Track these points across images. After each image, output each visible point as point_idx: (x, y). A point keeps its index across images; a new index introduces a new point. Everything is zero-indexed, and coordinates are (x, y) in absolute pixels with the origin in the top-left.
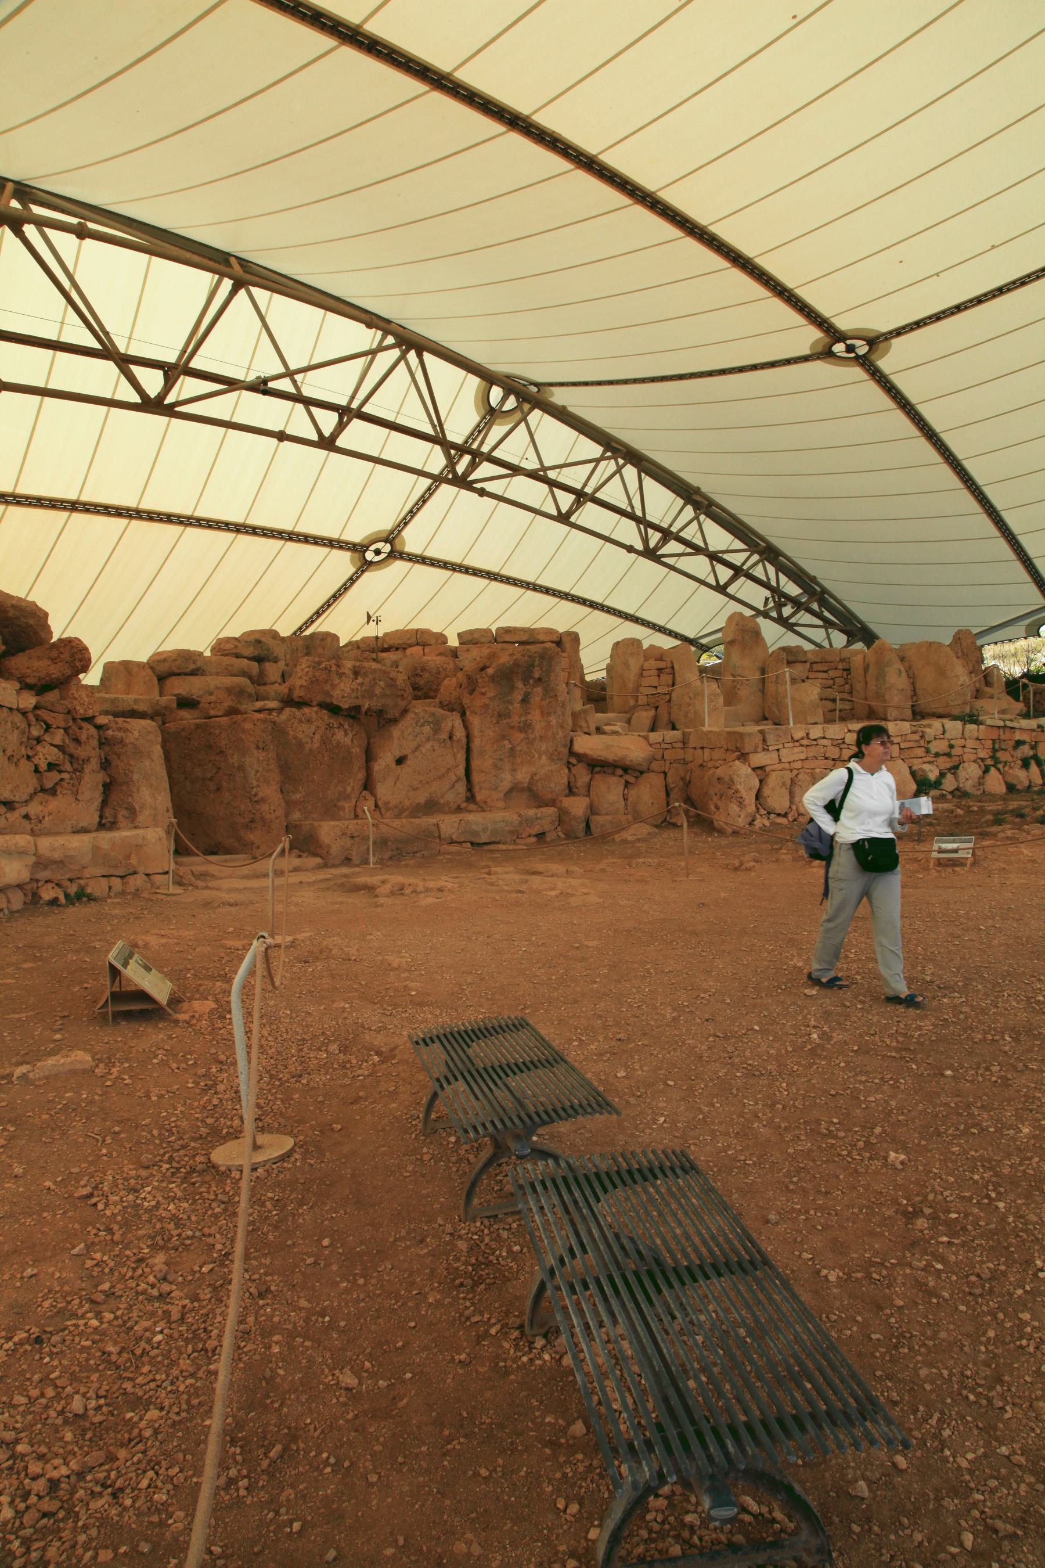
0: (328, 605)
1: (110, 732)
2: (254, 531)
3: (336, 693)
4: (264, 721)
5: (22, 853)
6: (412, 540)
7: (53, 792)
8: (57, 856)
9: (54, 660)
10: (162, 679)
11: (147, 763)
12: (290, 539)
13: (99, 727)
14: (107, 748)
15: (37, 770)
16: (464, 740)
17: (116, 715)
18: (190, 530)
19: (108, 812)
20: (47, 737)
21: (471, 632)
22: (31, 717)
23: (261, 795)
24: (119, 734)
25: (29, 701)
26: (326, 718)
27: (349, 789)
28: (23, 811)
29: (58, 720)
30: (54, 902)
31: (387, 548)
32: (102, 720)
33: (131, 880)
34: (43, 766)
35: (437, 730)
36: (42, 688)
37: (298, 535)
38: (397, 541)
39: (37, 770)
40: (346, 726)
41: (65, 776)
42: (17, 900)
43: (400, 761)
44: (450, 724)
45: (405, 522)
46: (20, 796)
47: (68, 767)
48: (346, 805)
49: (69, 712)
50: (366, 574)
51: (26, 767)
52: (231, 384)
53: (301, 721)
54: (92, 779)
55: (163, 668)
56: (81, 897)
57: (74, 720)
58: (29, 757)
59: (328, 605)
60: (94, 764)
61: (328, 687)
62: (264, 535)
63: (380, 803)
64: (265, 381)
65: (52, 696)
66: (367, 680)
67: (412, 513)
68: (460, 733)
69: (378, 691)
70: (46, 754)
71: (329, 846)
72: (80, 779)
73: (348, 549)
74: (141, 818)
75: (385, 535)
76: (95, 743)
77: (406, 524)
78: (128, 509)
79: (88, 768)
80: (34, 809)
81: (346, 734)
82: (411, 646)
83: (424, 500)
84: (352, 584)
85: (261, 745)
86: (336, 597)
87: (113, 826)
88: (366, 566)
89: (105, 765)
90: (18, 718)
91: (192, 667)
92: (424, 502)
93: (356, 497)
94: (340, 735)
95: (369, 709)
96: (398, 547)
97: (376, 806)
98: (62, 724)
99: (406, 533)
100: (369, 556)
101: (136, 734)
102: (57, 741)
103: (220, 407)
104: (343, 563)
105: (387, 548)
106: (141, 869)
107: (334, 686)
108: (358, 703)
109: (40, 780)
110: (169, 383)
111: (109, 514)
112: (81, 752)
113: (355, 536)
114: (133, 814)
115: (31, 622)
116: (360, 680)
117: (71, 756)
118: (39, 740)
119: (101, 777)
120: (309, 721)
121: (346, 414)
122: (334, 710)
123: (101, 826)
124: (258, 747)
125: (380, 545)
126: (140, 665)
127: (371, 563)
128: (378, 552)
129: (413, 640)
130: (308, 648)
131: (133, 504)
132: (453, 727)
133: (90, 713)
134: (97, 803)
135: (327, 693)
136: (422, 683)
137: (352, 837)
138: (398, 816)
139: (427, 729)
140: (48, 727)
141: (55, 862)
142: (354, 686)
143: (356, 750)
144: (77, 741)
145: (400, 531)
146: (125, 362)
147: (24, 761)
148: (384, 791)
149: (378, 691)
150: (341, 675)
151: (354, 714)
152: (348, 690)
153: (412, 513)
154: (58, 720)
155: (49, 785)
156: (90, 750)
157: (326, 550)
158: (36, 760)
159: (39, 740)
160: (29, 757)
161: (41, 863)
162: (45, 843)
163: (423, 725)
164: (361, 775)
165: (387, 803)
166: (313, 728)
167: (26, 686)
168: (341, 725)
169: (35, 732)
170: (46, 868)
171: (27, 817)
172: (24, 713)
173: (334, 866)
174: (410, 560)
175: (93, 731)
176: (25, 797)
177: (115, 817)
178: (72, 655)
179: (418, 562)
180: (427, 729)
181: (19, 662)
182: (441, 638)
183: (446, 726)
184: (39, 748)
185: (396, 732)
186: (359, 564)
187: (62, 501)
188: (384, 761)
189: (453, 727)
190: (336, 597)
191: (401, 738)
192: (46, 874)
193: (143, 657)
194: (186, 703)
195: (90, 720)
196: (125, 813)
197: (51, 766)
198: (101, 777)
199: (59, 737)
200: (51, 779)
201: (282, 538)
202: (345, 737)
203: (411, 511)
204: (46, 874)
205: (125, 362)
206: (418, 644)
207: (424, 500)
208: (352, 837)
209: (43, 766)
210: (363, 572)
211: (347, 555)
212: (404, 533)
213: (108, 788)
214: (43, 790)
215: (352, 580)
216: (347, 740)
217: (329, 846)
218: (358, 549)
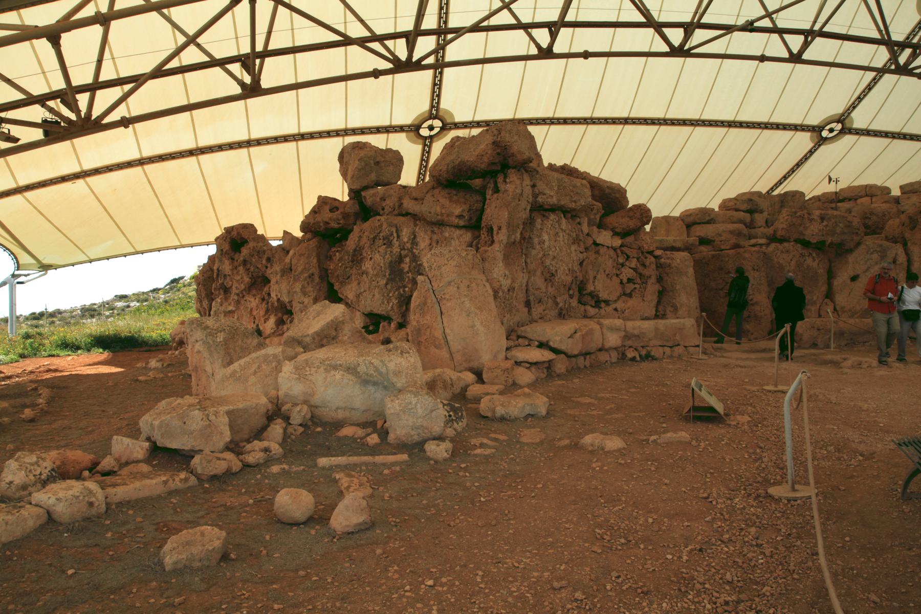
0: (792, 171)
1: (663, 260)
3: (808, 232)
4: (758, 252)
5: (618, 330)
6: (859, 119)
7: (630, 295)
8: (636, 332)
9: (631, 218)
10: (689, 226)
11: (685, 279)
12: (766, 128)
13: (656, 257)
14: (660, 270)
15: (621, 283)
16: (905, 264)
17: (665, 249)
18: (698, 129)
19: (661, 308)
20: (627, 263)
21: (911, 184)
22: (618, 251)
23: (755, 300)
24: (668, 261)
25: (617, 242)
26: (800, 249)
27: (815, 298)
28: (614, 306)
29: (633, 253)
30: (633, 359)
31: (839, 126)
32: (658, 253)
33: (676, 349)
34: (625, 280)
35: (883, 258)
36: (624, 234)
37: (772, 124)
38: (846, 121)
39: (621, 283)
40: (814, 255)
41: (637, 286)
42: (614, 356)
44: (894, 252)
45: (853, 106)
46: (613, 297)
47: (638, 281)
48: (813, 308)
49: (640, 248)
50: (822, 147)
51: (616, 281)
52: (728, 29)
53: (782, 252)
54: (652, 288)
55: (690, 220)
56: (648, 357)
57: (642, 253)
58: (617, 275)
59: (792, 171)
60: (653, 279)
61: (801, 229)
62: (748, 127)
63: (838, 308)
64: (752, 23)
65: (630, 239)
66: (831, 223)
67: (860, 99)
68: (902, 258)
69: (838, 230)
70: (627, 273)
71: (802, 335)
72: (645, 288)
73: (809, 131)
74: (680, 312)
75: (837, 117)
76: (654, 266)
77: (854, 108)
78: (659, 119)
79: (650, 281)
80: (619, 305)
81: (814, 260)
82: (861, 197)
83: (869, 88)
84: (811, 155)
85: (756, 268)
86: (798, 165)
87: (663, 317)
89: (660, 280)
90: (612, 252)
91: (708, 218)
92: (870, 89)
93: (814, 93)
94: (809, 261)
95: (832, 243)
96: (848, 125)
97: (835, 309)
98: (636, 256)
99: (854, 115)
100: (825, 134)
101: (678, 261)
102: (633, 265)
104: (804, 140)
105: (839, 126)
106: (682, 343)
107: (806, 228)
108: (823, 238)
109: (623, 288)
110: (688, 35)
111: (647, 124)
112: (646, 272)
113: (813, 120)
114: (675, 309)
115: (618, 195)
116: (825, 223)
117: (640, 274)
118: (623, 265)
119: (657, 287)
120: (788, 252)
121: (809, 35)
122: (806, 244)
123: (657, 317)
124: (754, 269)
125: (833, 125)
126: (674, 218)
127: (826, 139)
128: (831, 130)
129: (863, 193)
130: (782, 202)
131: (661, 116)
132: (896, 254)
133: (651, 249)
134: (655, 303)
135: (801, 233)
136: (870, 223)
137: (819, 330)
138: (851, 317)
139: (875, 256)
140: (628, 257)
141: (635, 336)
142: (821, 227)
143: (821, 271)
144: (644, 265)
145: (849, 114)
146: (659, 27)
147: (614, 278)
148: (840, 299)
149: (838, 230)
150: (811, 220)
151: (820, 247)
152: (816, 230)
153: (860, 99)
154: (633, 253)
155: (628, 291)
156: (651, 271)
157: (792, 133)
158: (621, 277)
159: (623, 265)
160: (617, 275)
161: (627, 336)
162: (630, 324)
163: (872, 253)
164: (824, 288)
165: (843, 308)
166: (791, 257)
167: (616, 234)
168: (810, 254)
169: (621, 260)
170: (629, 339)
171: (616, 309)
172: (615, 249)
173: (804, 348)
174: (857, 134)
175: (653, 259)
176: (615, 298)
177: (665, 311)
178: (641, 215)
179: (863, 134)
180: (875, 256)
181: (612, 220)
182: (886, 190)
183: (891, 254)
184: (623, 270)
185: (851, 258)
186: (816, 140)
187: (619, 119)
188: (842, 278)
189: (896, 254)
190: (798, 165)
192: (628, 343)
193: (677, 213)
194: (704, 241)
195: (651, 253)
196: (671, 309)
197: (630, 280)
198: (657, 287)
199: (634, 263)
201: (760, 128)
202: (813, 262)
203: (859, 98)
204: (628, 343)
205: (659, 27)
206: (867, 195)
207: (869, 88)
208: (819, 330)
209: (625, 280)
210: (820, 146)
211: (808, 134)
212: (853, 115)
213: (661, 294)
214: (625, 294)
215: (811, 152)
216: (815, 265)
217: (802, 335)
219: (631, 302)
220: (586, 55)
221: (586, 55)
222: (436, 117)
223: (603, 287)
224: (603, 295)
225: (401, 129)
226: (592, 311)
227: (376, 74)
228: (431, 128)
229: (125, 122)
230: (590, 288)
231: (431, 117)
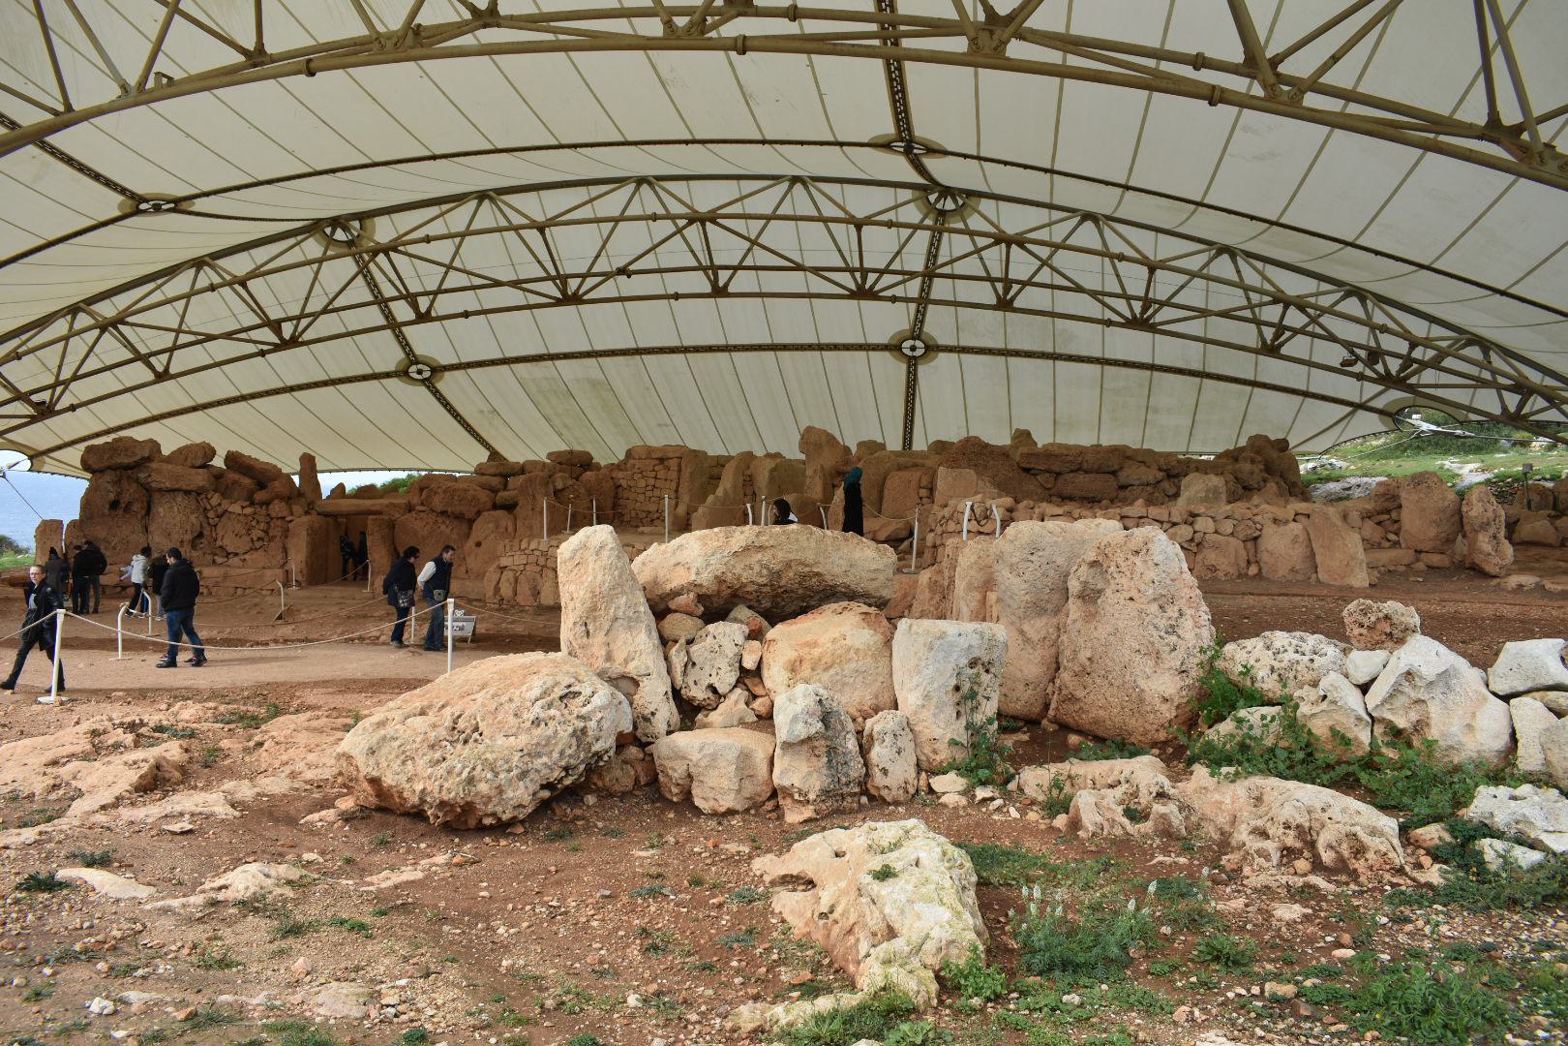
2: (785, 347)
36: (261, 504)
43: (478, 544)
50: (921, 369)
68: (510, 529)
70: (256, 533)
88: (912, 363)
99: (926, 329)
103: (608, 289)
105: (919, 344)
125: (910, 343)
128: (913, 348)
183: (503, 523)
191: (482, 528)
199: (262, 526)
200: (258, 544)
202: (446, 528)
218: (894, 348)
219: (255, 555)
220: (466, 314)
221: (466, 314)
222: (417, 363)
223: (229, 542)
224: (230, 549)
225: (388, 375)
226: (219, 560)
227: (262, 353)
228: (420, 372)
229: (73, 408)
230: (219, 543)
231: (412, 363)
